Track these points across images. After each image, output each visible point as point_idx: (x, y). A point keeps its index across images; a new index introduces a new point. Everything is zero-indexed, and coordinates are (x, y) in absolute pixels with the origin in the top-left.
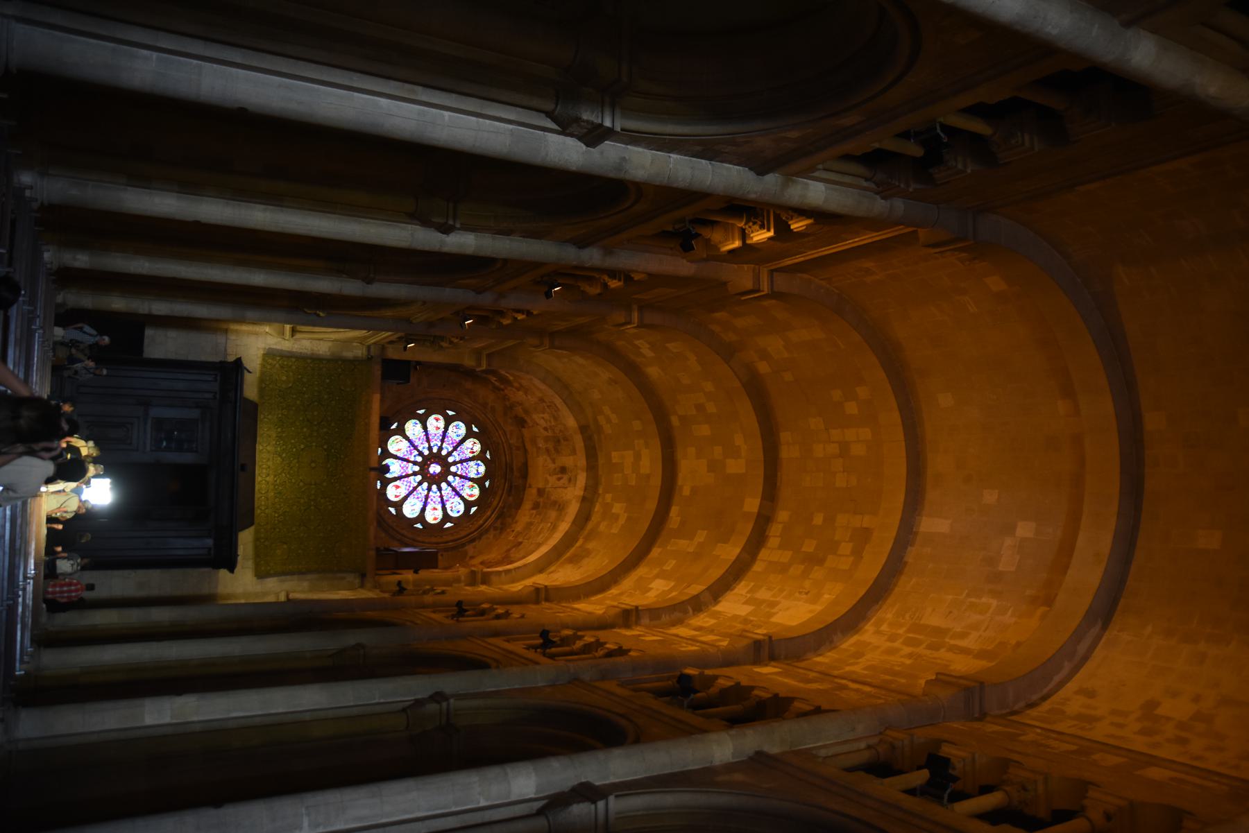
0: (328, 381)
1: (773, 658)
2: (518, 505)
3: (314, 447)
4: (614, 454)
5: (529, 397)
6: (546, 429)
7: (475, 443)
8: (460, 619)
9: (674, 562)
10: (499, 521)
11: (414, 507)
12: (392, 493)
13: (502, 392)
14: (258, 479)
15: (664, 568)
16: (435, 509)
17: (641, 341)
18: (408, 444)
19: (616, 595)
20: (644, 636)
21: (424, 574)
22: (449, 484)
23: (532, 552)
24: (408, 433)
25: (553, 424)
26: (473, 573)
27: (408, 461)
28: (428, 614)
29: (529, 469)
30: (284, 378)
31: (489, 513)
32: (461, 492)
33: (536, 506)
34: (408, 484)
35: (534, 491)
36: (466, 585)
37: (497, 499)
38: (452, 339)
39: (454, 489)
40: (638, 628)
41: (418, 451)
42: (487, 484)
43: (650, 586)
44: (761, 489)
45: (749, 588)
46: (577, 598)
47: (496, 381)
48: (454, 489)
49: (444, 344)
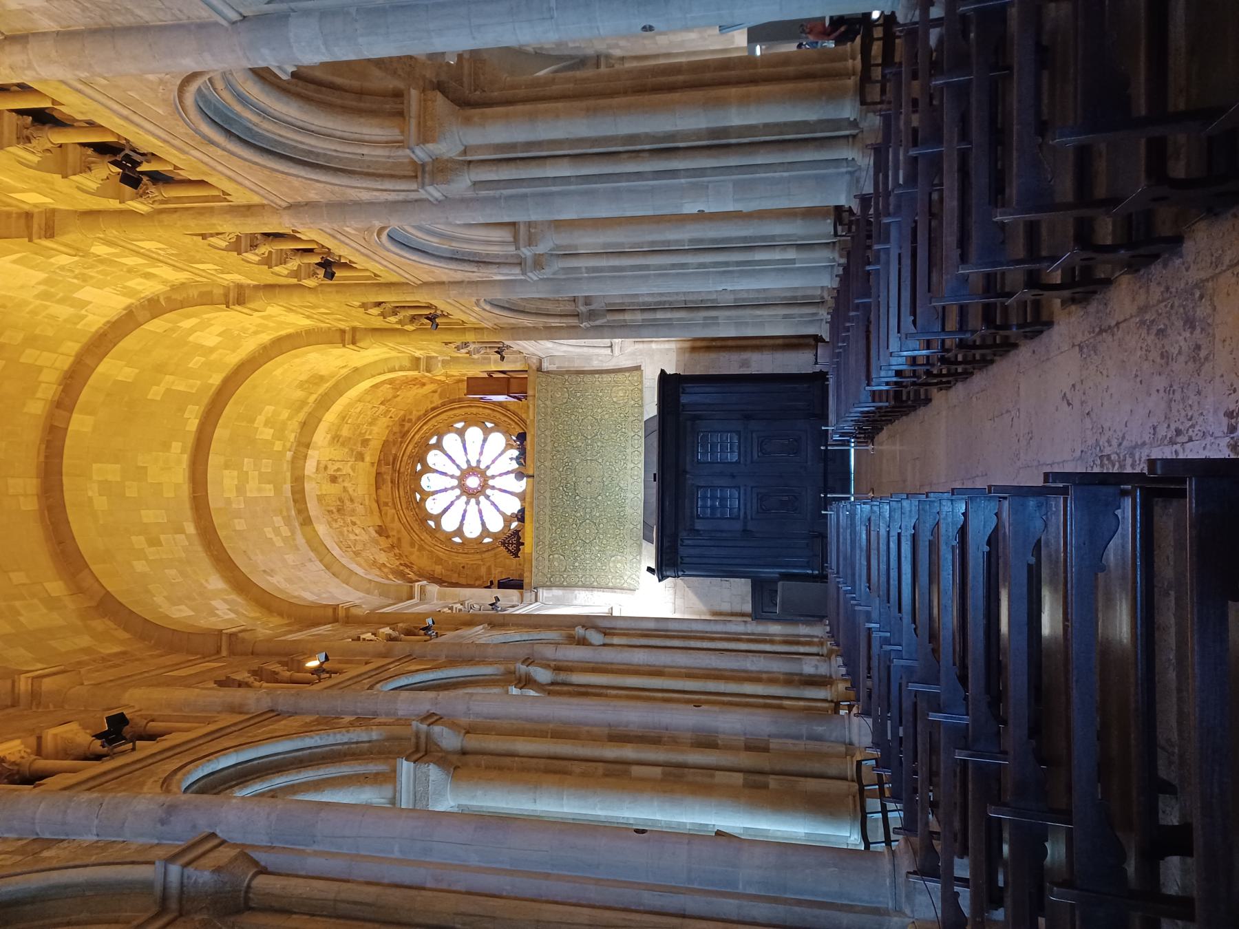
0: (577, 564)
1: (28, 216)
2: (386, 444)
4: (272, 494)
5: (371, 557)
6: (354, 524)
8: (432, 311)
10: (406, 428)
17: (226, 617)
19: (263, 332)
20: (216, 270)
23: (367, 392)
25: (345, 529)
26: (429, 371)
28: (471, 319)
29: (373, 482)
30: (619, 565)
31: (417, 437)
32: (446, 458)
35: (368, 459)
36: (437, 357)
38: (450, 611)
40: (227, 282)
41: (490, 501)
42: (419, 467)
43: (220, 339)
44: (68, 442)
45: (83, 322)
46: (309, 332)
48: (453, 461)
49: (459, 606)
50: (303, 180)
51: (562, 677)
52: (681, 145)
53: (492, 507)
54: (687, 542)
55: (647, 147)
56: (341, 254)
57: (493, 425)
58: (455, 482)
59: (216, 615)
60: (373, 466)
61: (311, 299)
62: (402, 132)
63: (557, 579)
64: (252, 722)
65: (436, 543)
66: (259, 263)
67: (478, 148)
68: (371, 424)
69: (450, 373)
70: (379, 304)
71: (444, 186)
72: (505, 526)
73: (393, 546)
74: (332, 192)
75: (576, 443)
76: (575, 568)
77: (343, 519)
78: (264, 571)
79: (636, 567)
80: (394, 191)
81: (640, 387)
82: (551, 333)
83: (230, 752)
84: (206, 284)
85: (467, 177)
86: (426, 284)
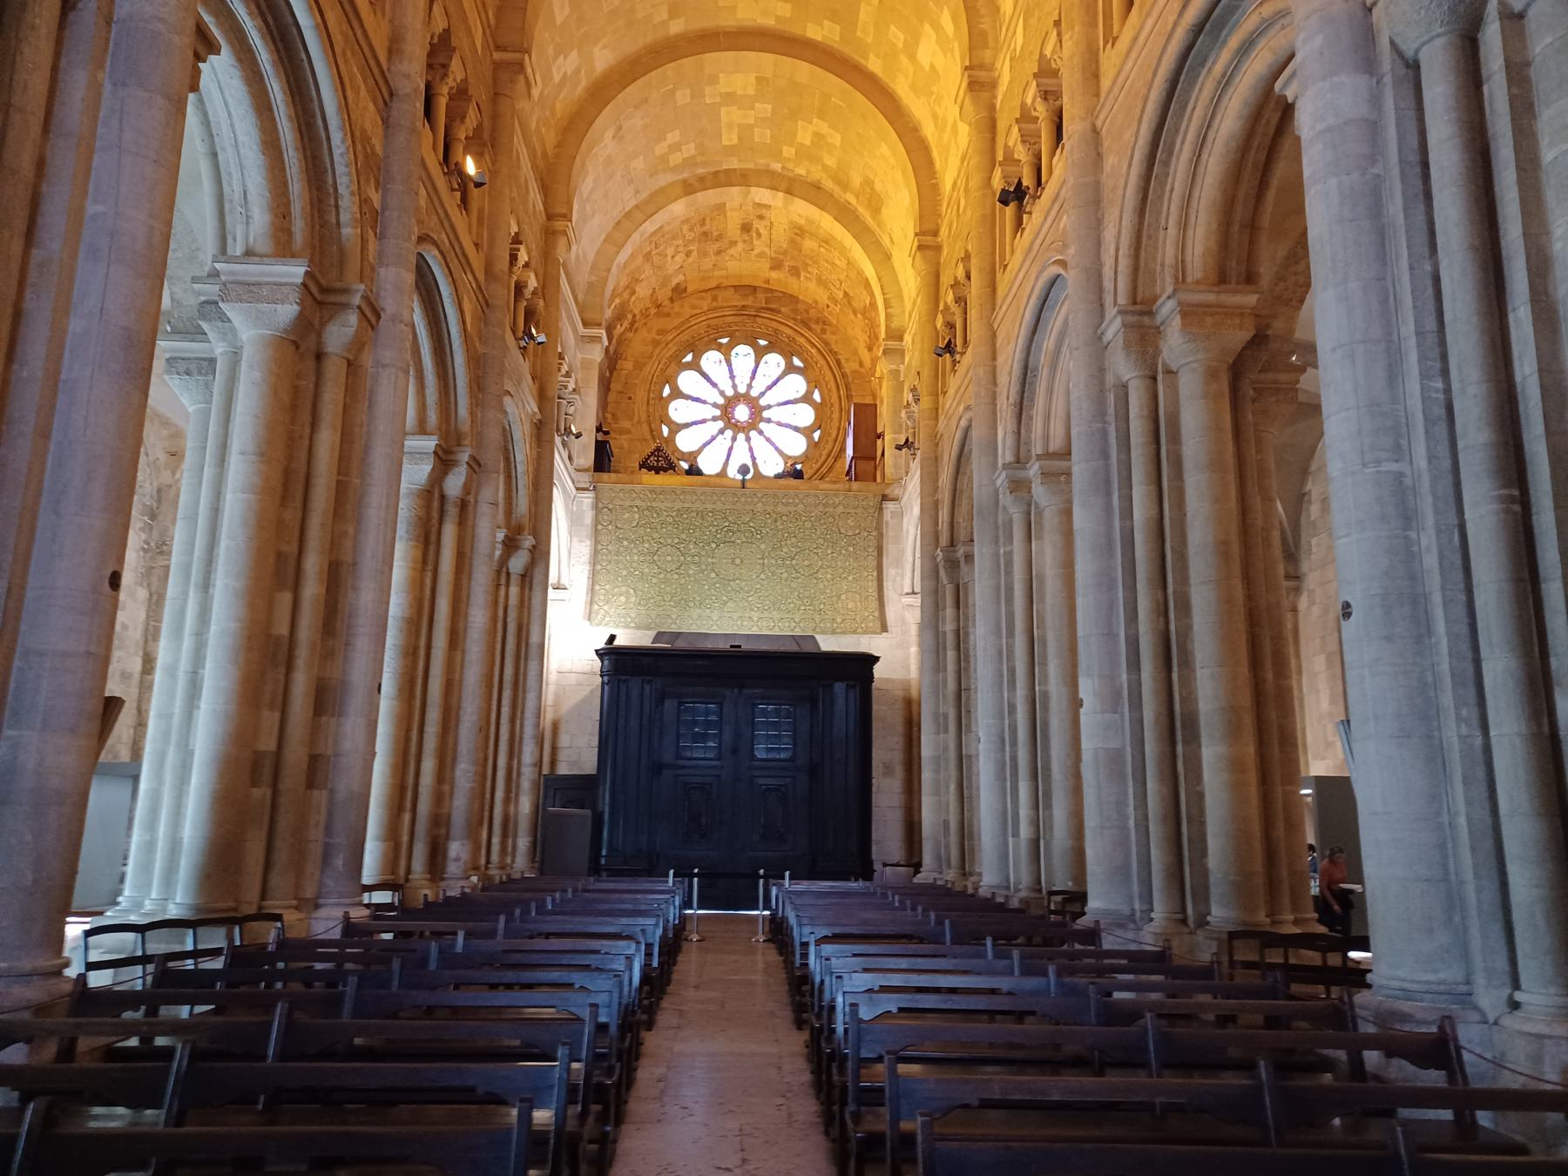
2: (794, 299)
3: (714, 560)
4: (725, 142)
5: (643, 276)
6: (688, 254)
8: (959, 349)
9: (892, 28)
10: (814, 326)
13: (638, 317)
14: (755, 631)
15: (900, 45)
19: (936, 126)
20: (1015, 50)
21: (884, 422)
23: (860, 273)
24: (694, 448)
26: (885, 352)
28: (948, 402)
30: (623, 599)
31: (802, 340)
32: (774, 378)
33: (795, 272)
35: (774, 275)
36: (903, 363)
37: (782, 328)
38: (563, 372)
40: (999, 67)
42: (763, 342)
43: (927, 67)
48: (769, 388)
49: (571, 386)
50: (1132, 144)
51: (452, 511)
52: (1175, 676)
53: (709, 438)
54: (647, 688)
55: (1172, 627)
56: (1034, 215)
57: (816, 439)
58: (742, 389)
59: (556, 58)
60: (764, 282)
61: (975, 183)
62: (1198, 282)
63: (605, 517)
64: (372, 62)
65: (663, 362)
66: (1023, 105)
67: (1174, 389)
69: (885, 384)
70: (968, 277)
71: (1121, 341)
72: (683, 453)
73: (659, 306)
74: (1115, 187)
75: (786, 544)
76: (620, 540)
77: (693, 240)
78: (620, 128)
79: (620, 622)
80: (1116, 273)
81: (859, 630)
82: (930, 509)
83: (315, 18)
84: (997, 40)
85: (1134, 375)
86: (994, 335)
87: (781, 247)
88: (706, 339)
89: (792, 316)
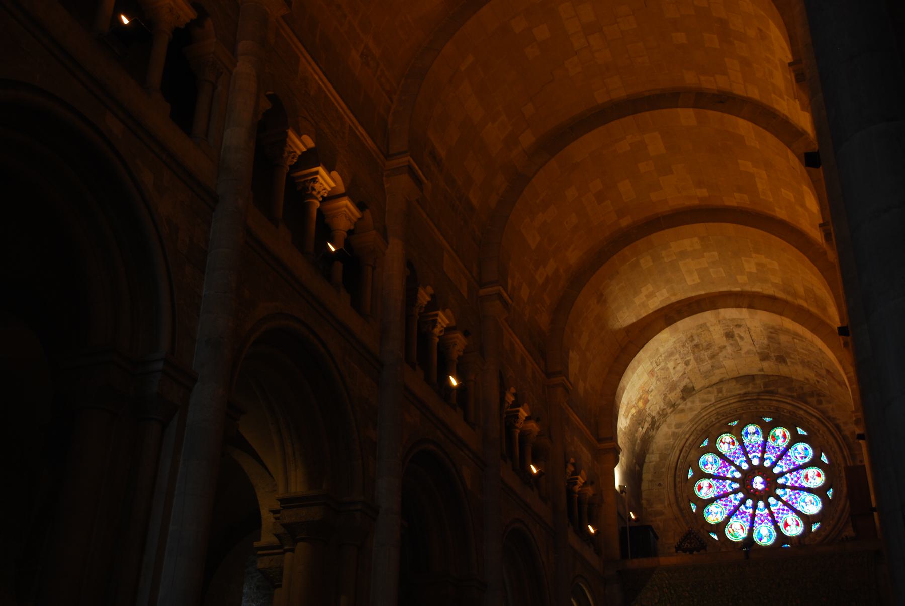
2: (787, 381)
5: (652, 387)
7: (722, 441)
10: (810, 400)
11: (813, 502)
12: (794, 529)
13: (656, 419)
15: (793, 200)
16: (807, 477)
18: (734, 517)
22: (774, 464)
24: (720, 518)
25: (677, 356)
27: (753, 516)
29: (742, 373)
31: (802, 413)
34: (781, 511)
35: (765, 364)
37: (782, 405)
39: (779, 458)
41: (740, 505)
42: (767, 420)
44: (665, 111)
47: (642, 428)
48: (779, 458)
58: (756, 462)
60: (759, 371)
68: (803, 362)
73: (673, 406)
78: (602, 295)
87: (764, 343)
88: (718, 425)
89: (789, 394)
